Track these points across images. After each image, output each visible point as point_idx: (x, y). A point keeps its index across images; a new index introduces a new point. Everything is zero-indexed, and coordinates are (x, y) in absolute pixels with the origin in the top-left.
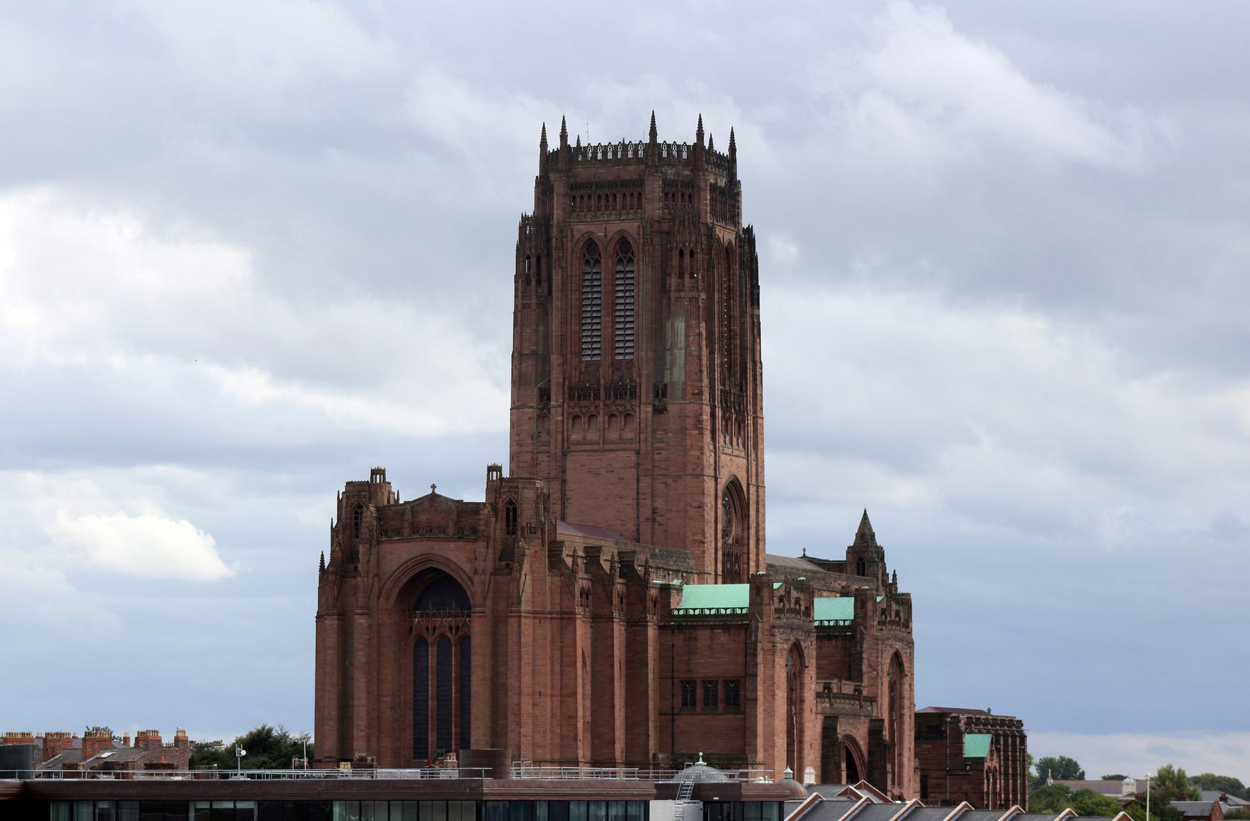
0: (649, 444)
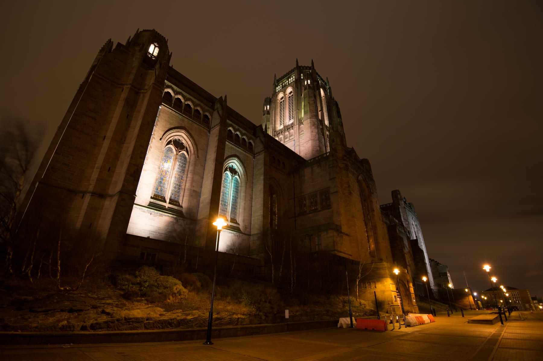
0: (298, 136)
